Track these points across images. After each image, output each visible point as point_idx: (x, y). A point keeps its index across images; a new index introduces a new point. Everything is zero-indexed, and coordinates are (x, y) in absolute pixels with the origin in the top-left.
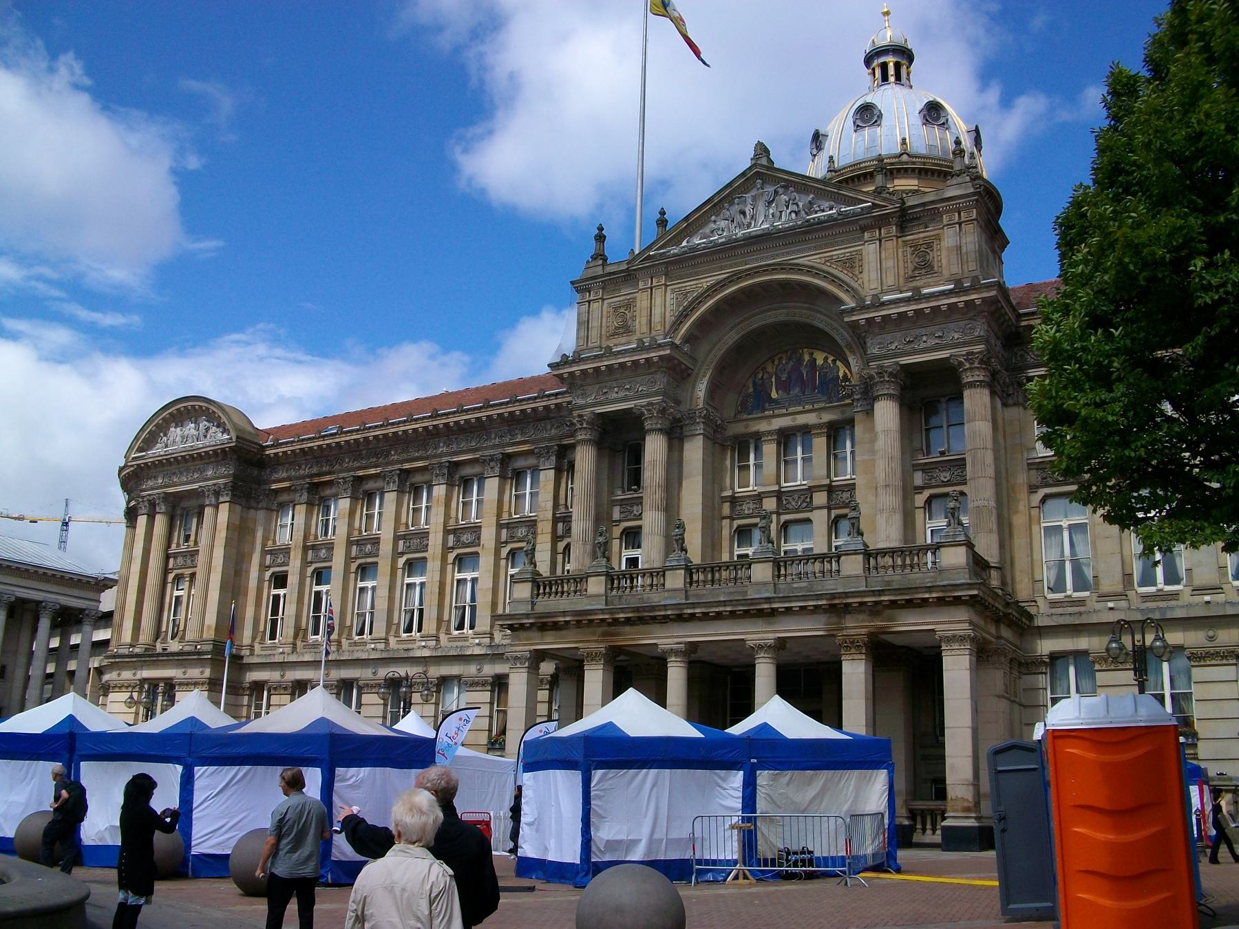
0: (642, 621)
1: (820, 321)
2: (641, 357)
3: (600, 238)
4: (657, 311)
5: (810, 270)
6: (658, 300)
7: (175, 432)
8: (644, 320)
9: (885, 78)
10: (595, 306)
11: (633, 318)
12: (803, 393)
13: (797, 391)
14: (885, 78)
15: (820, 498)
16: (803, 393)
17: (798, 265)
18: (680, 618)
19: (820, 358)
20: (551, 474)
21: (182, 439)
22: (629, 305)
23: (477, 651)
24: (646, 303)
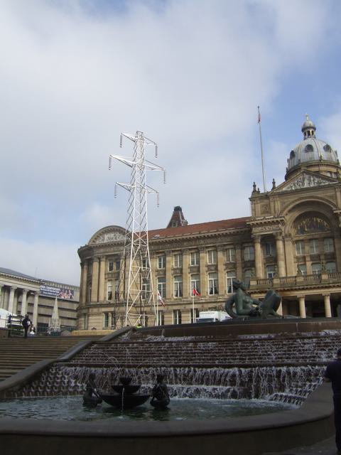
0: (292, 290)
1: (322, 211)
2: (275, 220)
3: (254, 186)
5: (321, 198)
7: (106, 236)
10: (256, 205)
13: (313, 229)
14: (309, 134)
15: (322, 257)
18: (303, 289)
19: (319, 220)
20: (240, 250)
21: (107, 238)
23: (221, 300)
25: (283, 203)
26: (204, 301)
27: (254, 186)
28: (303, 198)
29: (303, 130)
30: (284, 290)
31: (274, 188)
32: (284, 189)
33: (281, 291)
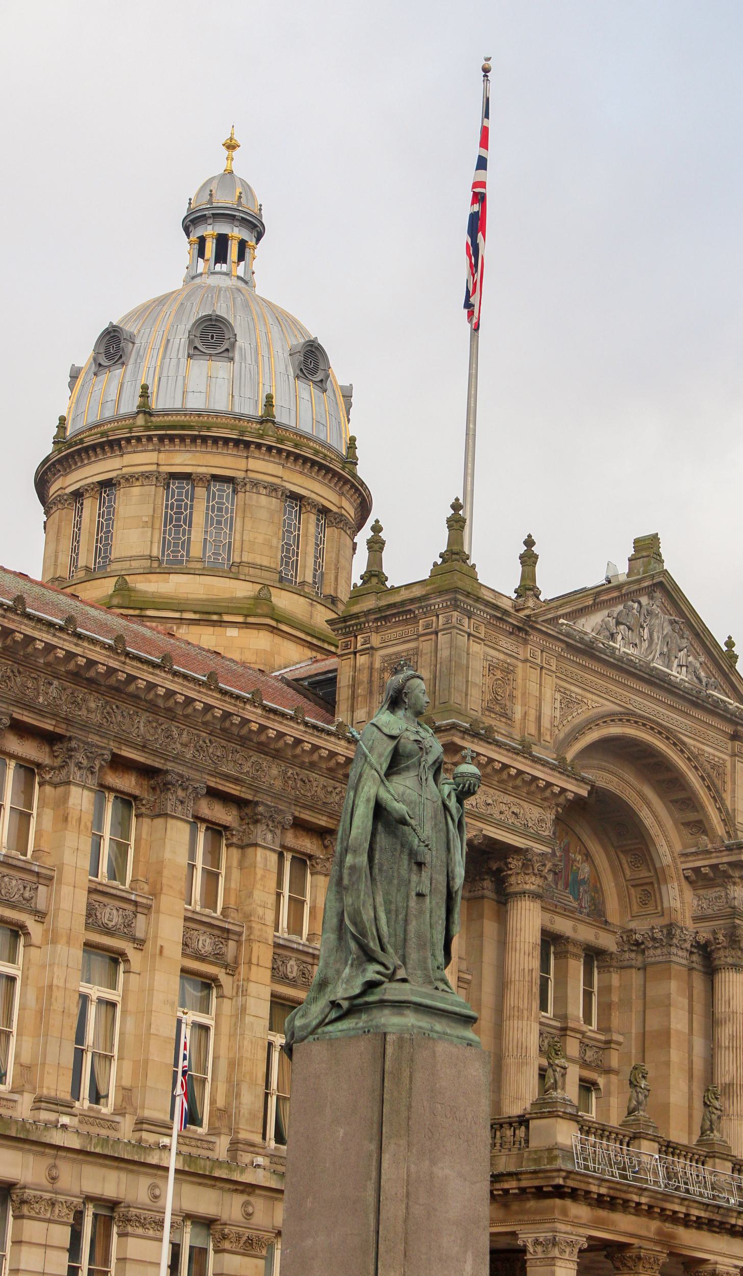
3: (457, 523)
4: (547, 710)
5: (693, 758)
6: (548, 693)
8: (532, 714)
9: (221, 256)
11: (512, 697)
12: (556, 884)
14: (221, 256)
16: (556, 884)
17: (683, 743)
22: (508, 671)
24: (533, 688)
25: (568, 702)
26: (75, 1142)
27: (457, 523)
28: (627, 717)
29: (191, 222)
30: (686, 1222)
31: (528, 587)
32: (589, 625)
33: (674, 1218)
